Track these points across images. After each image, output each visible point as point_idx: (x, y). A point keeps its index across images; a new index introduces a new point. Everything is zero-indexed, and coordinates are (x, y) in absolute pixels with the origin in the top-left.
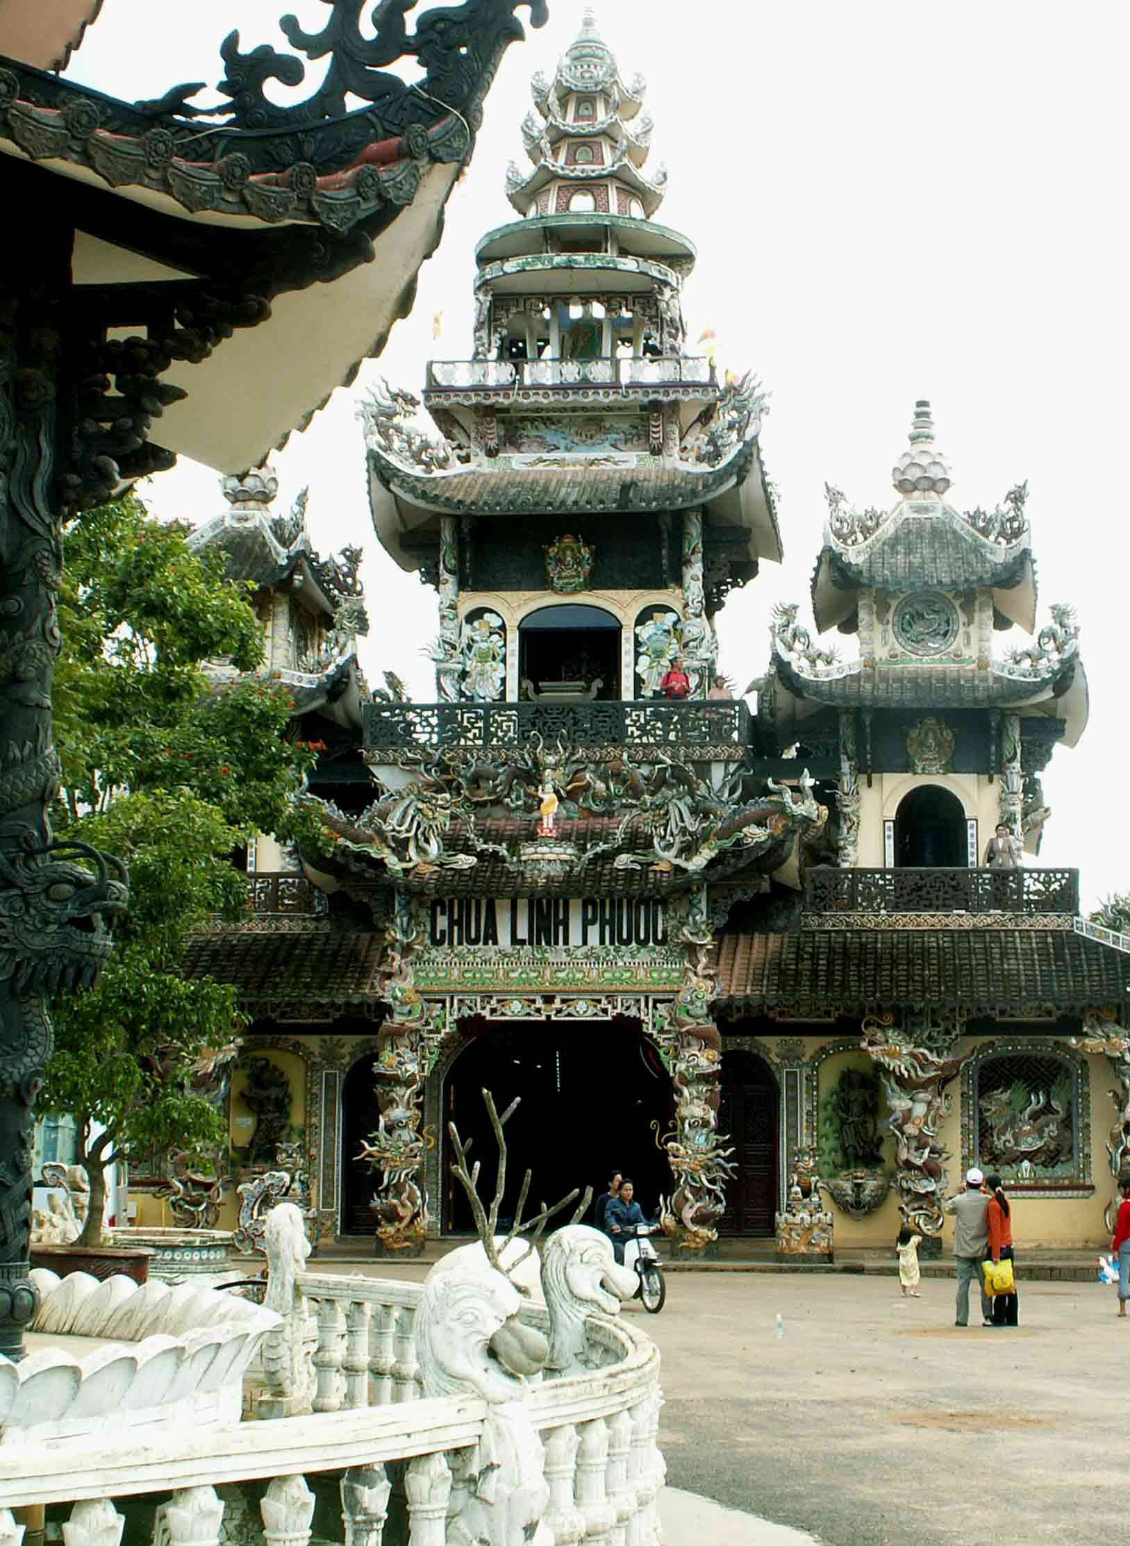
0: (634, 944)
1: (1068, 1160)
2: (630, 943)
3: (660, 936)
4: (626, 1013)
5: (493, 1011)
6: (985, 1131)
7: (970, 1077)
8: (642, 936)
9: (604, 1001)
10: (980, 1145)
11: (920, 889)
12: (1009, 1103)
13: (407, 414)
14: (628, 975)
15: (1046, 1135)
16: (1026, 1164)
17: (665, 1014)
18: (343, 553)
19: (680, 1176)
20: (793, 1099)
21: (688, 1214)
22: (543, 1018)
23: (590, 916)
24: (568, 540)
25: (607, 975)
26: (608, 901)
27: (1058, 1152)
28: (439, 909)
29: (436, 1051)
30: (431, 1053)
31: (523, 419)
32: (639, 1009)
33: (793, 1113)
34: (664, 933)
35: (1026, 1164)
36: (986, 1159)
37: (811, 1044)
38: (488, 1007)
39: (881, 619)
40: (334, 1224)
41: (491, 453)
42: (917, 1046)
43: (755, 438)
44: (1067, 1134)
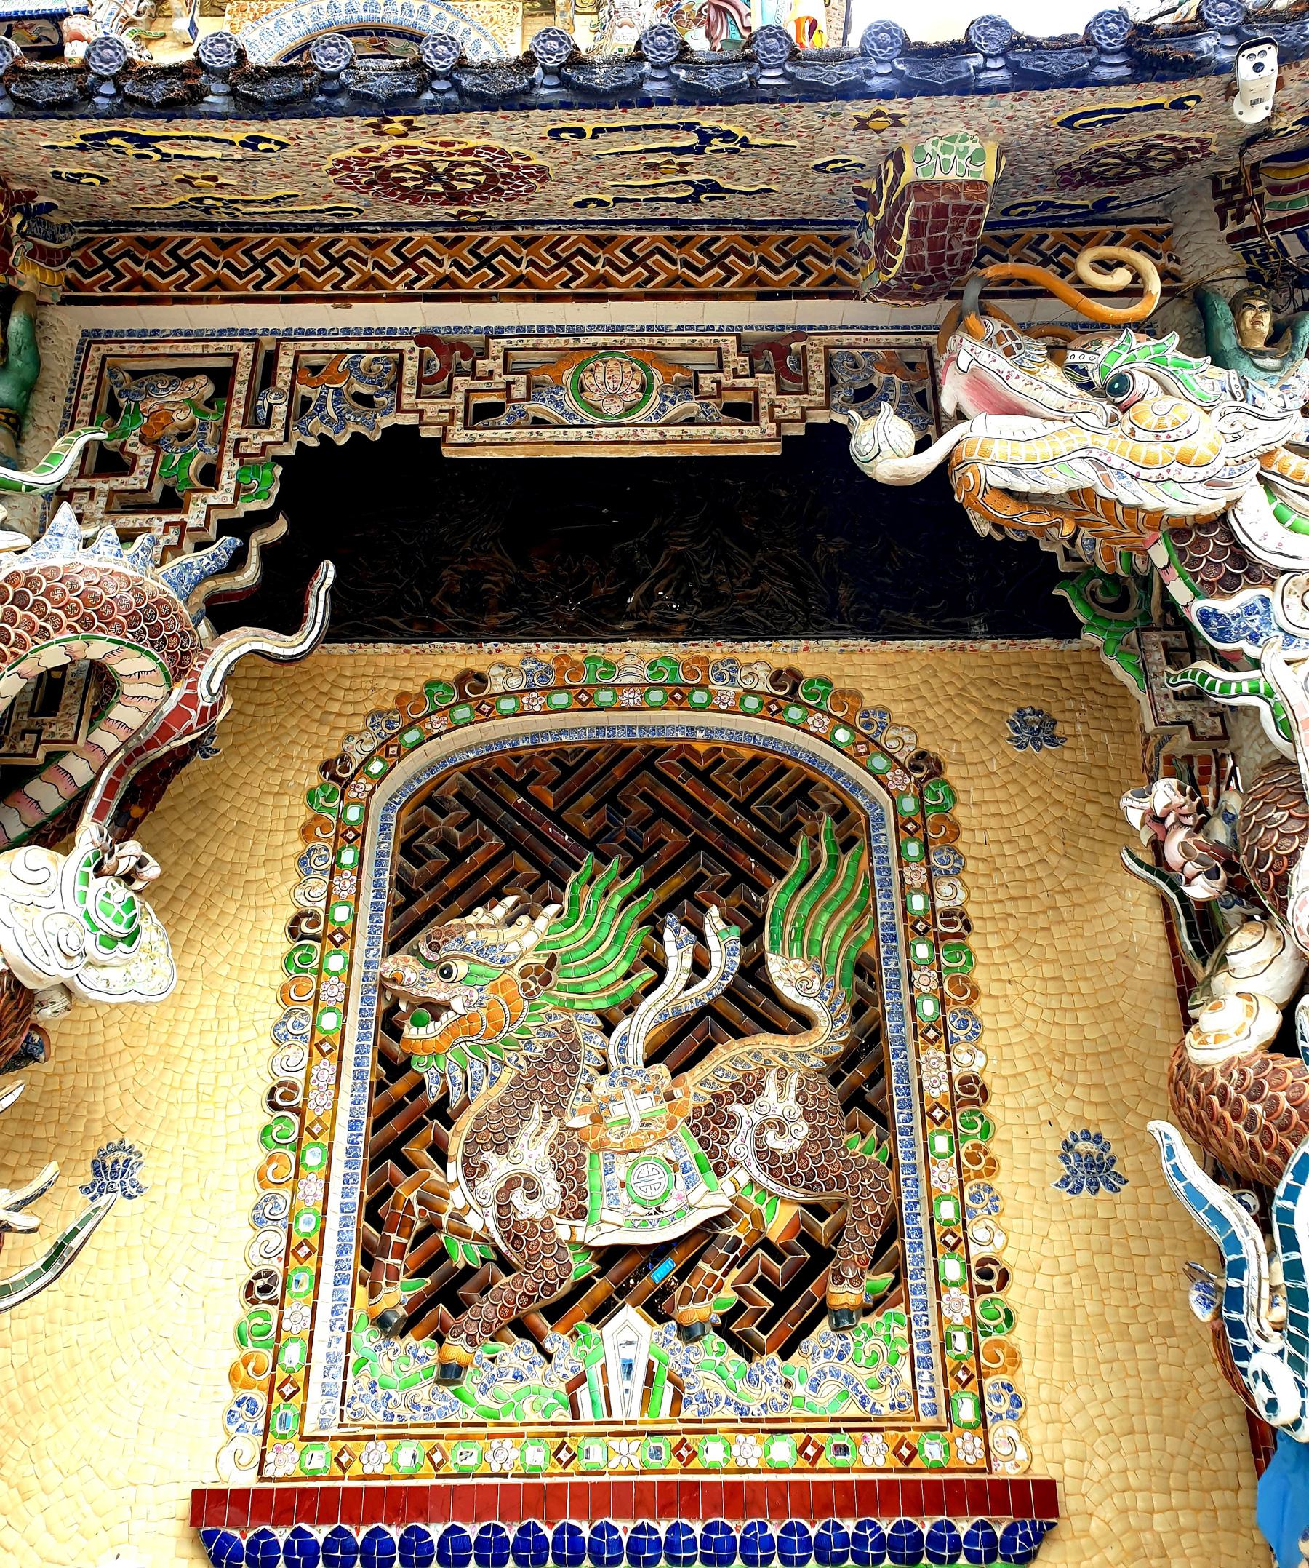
1: (875, 1305)
6: (406, 1122)
10: (372, 1213)
12: (543, 974)
15: (740, 1146)
27: (816, 1256)
44: (856, 1145)
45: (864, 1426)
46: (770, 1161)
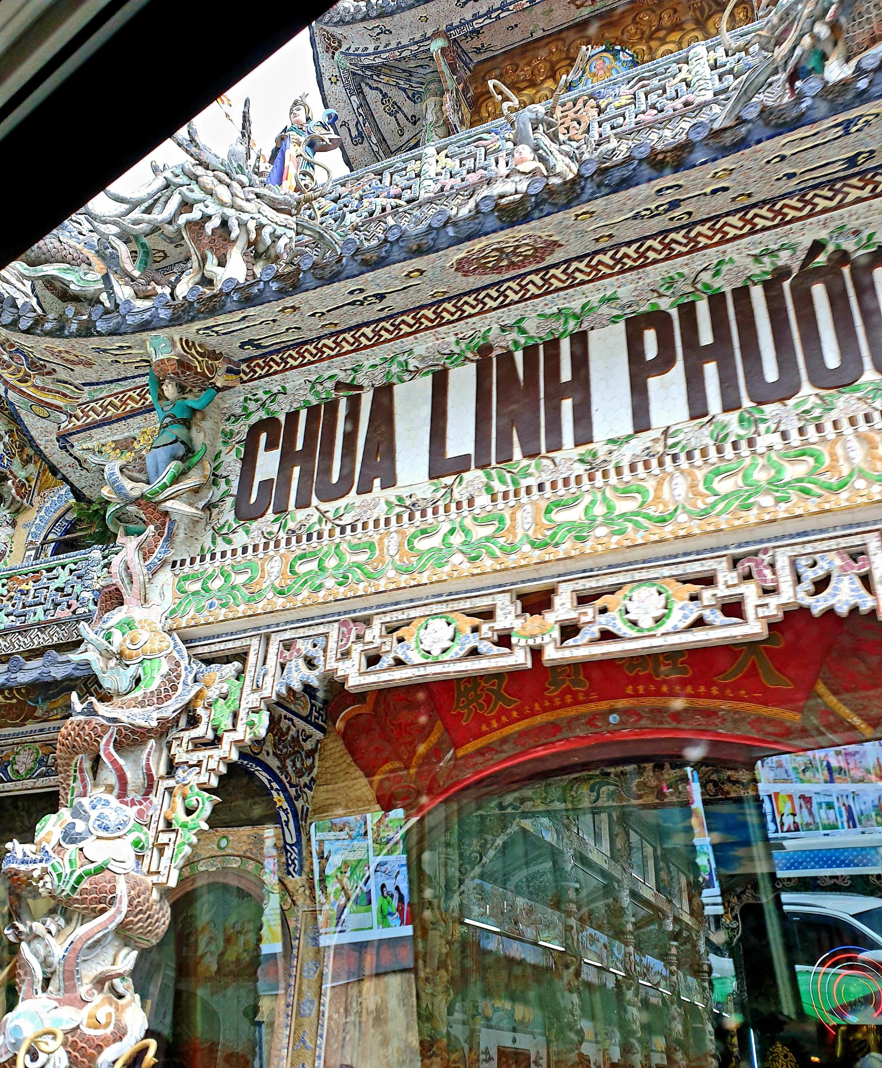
0: (807, 389)
2: (796, 389)
9: (726, 576)
22: (520, 658)
26: (703, 309)
28: (263, 437)
38: (357, 649)
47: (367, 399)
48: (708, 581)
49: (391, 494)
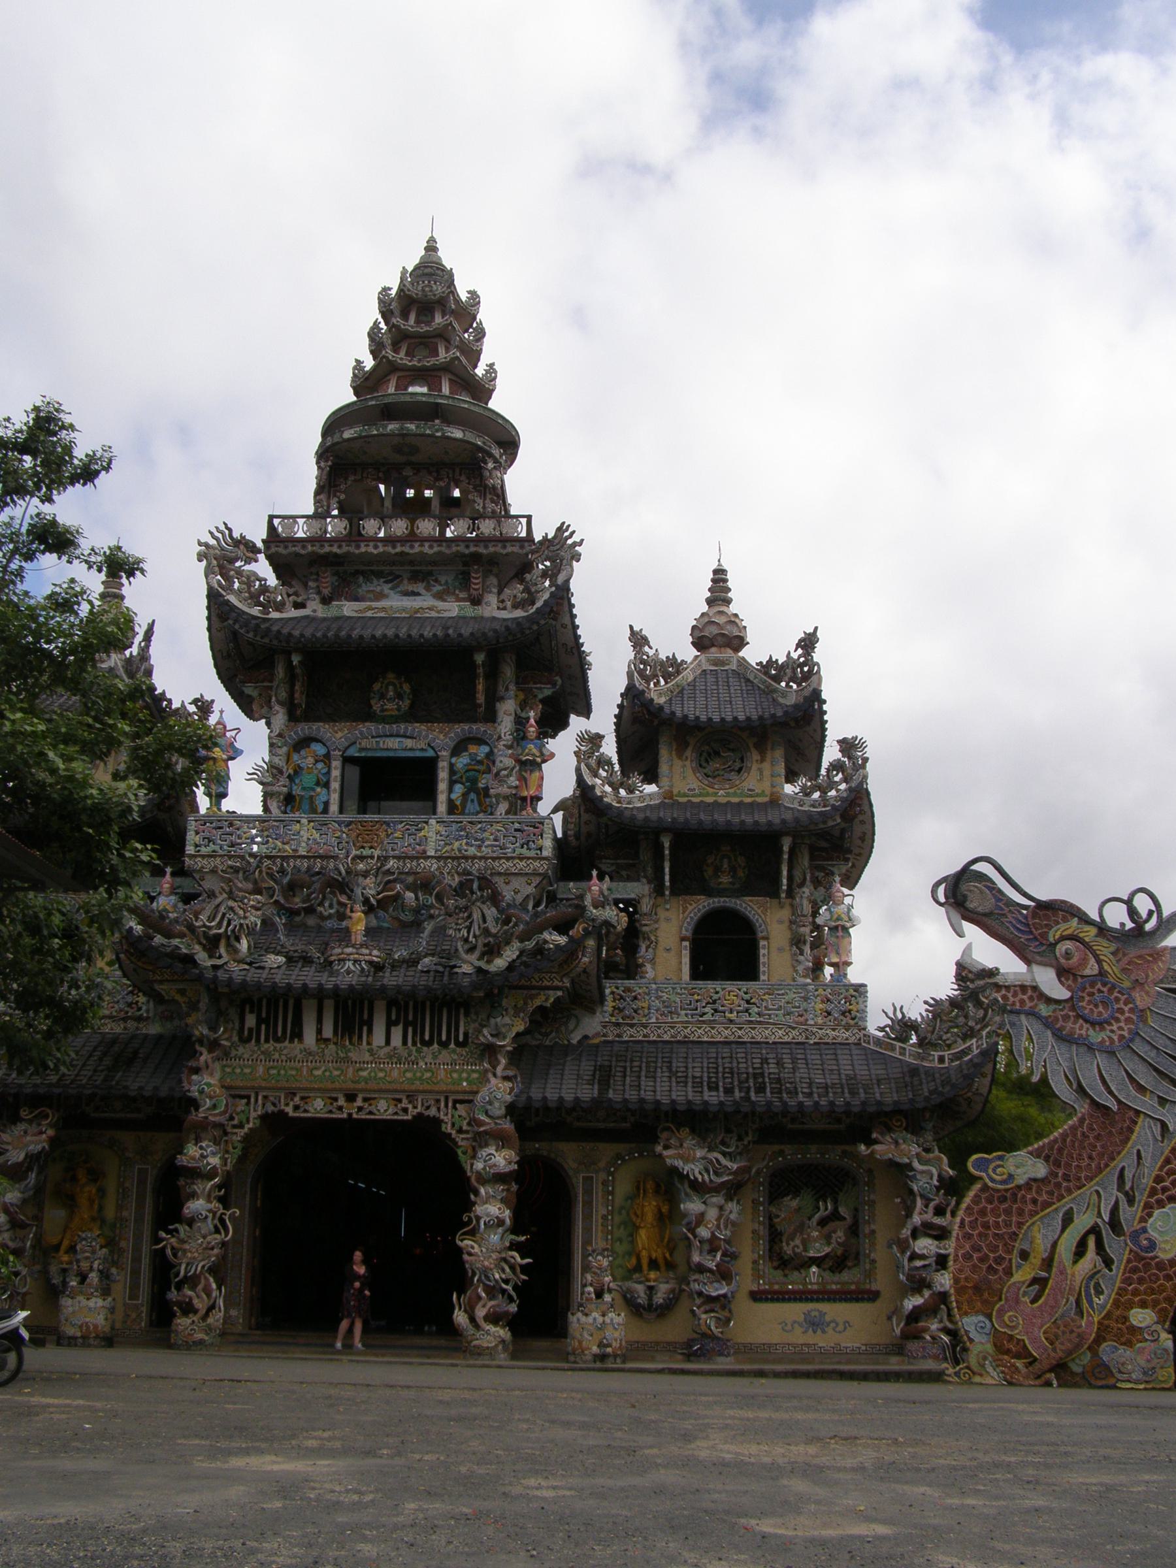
0: (436, 1045)
1: (855, 1266)
3: (461, 1039)
4: (427, 1113)
5: (296, 1108)
6: (775, 1236)
7: (761, 1184)
8: (444, 1038)
9: (405, 1101)
10: (770, 1250)
11: (714, 1002)
12: (798, 1210)
13: (248, 561)
14: (428, 1075)
15: (833, 1241)
16: (814, 1269)
17: (464, 1114)
18: (195, 702)
19: (474, 1274)
20: (588, 1204)
21: (480, 1313)
22: (345, 1116)
23: (394, 1017)
24: (391, 676)
25: (409, 1075)
26: (411, 1004)
29: (240, 1146)
30: (234, 1148)
31: (357, 573)
32: (439, 1109)
33: (588, 1217)
34: (466, 1035)
35: (814, 1269)
36: (776, 1264)
37: (607, 1151)
38: (291, 1104)
39: (680, 755)
40: (139, 1315)
41: (326, 601)
42: (711, 1150)
43: (567, 581)
45: (853, 1283)
46: (839, 1243)
47: (291, 1002)
48: (400, 1101)
49: (302, 1046)
